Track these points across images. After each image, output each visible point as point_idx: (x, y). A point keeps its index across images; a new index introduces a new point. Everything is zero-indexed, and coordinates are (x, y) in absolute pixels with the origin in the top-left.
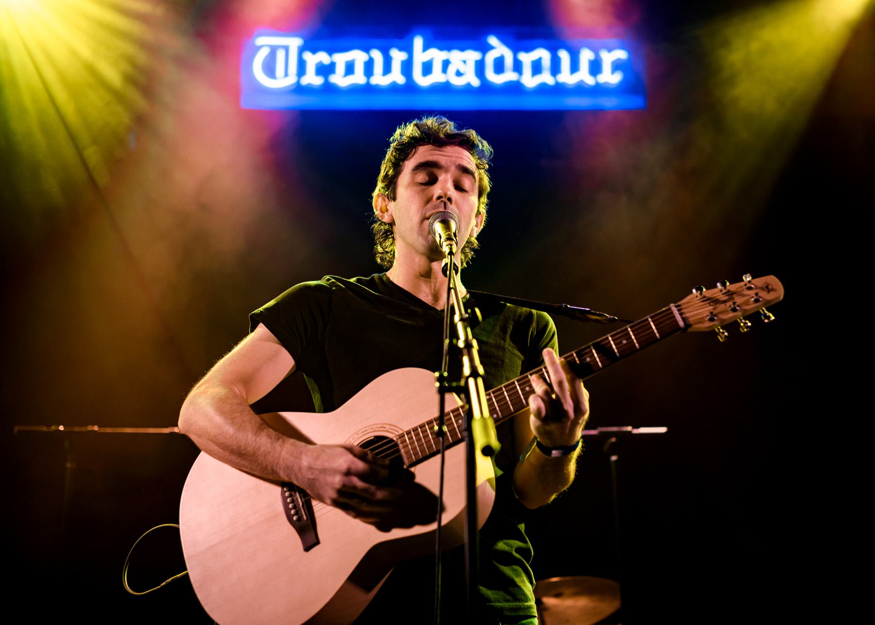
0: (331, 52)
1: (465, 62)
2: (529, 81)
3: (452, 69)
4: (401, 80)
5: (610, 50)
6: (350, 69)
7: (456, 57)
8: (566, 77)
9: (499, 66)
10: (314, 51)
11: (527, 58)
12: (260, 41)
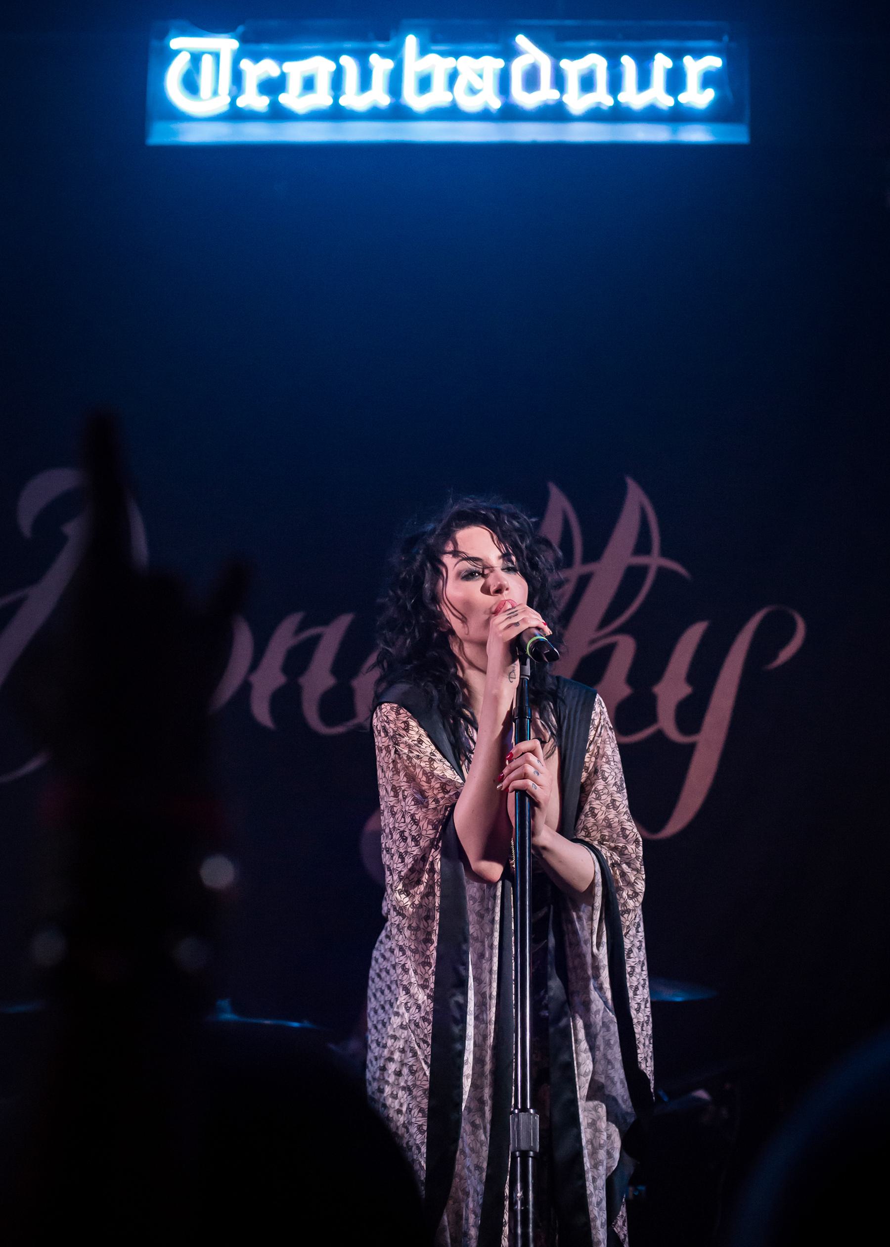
0: (281, 58)
3: (460, 84)
4: (384, 101)
5: (698, 54)
6: (309, 84)
7: (466, 64)
9: (531, 81)
10: (257, 58)
11: (573, 68)
12: (175, 43)
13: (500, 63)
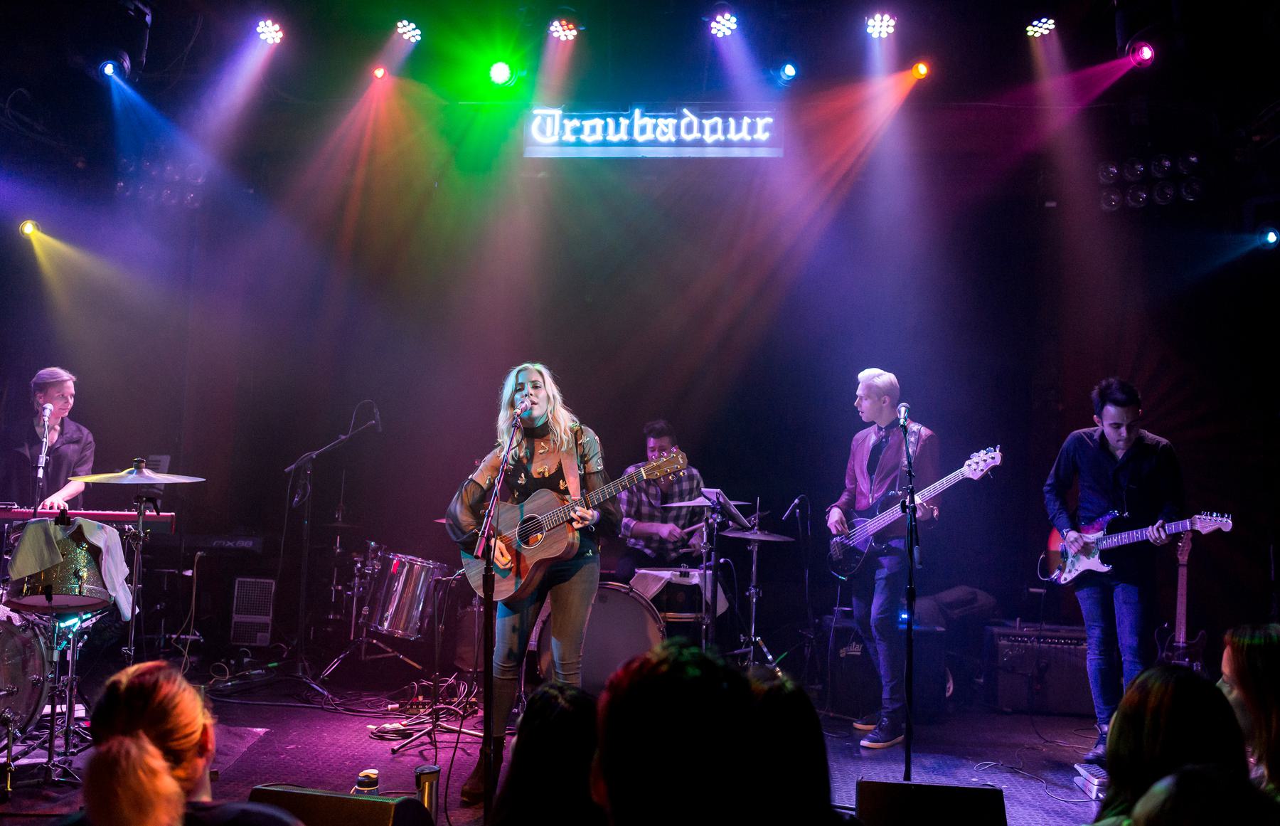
1: (667, 126)
2: (709, 138)
5: (763, 116)
6: (593, 130)
7: (661, 121)
8: (733, 136)
9: (689, 129)
10: (571, 118)
11: (707, 123)
12: (535, 112)
13: (675, 121)
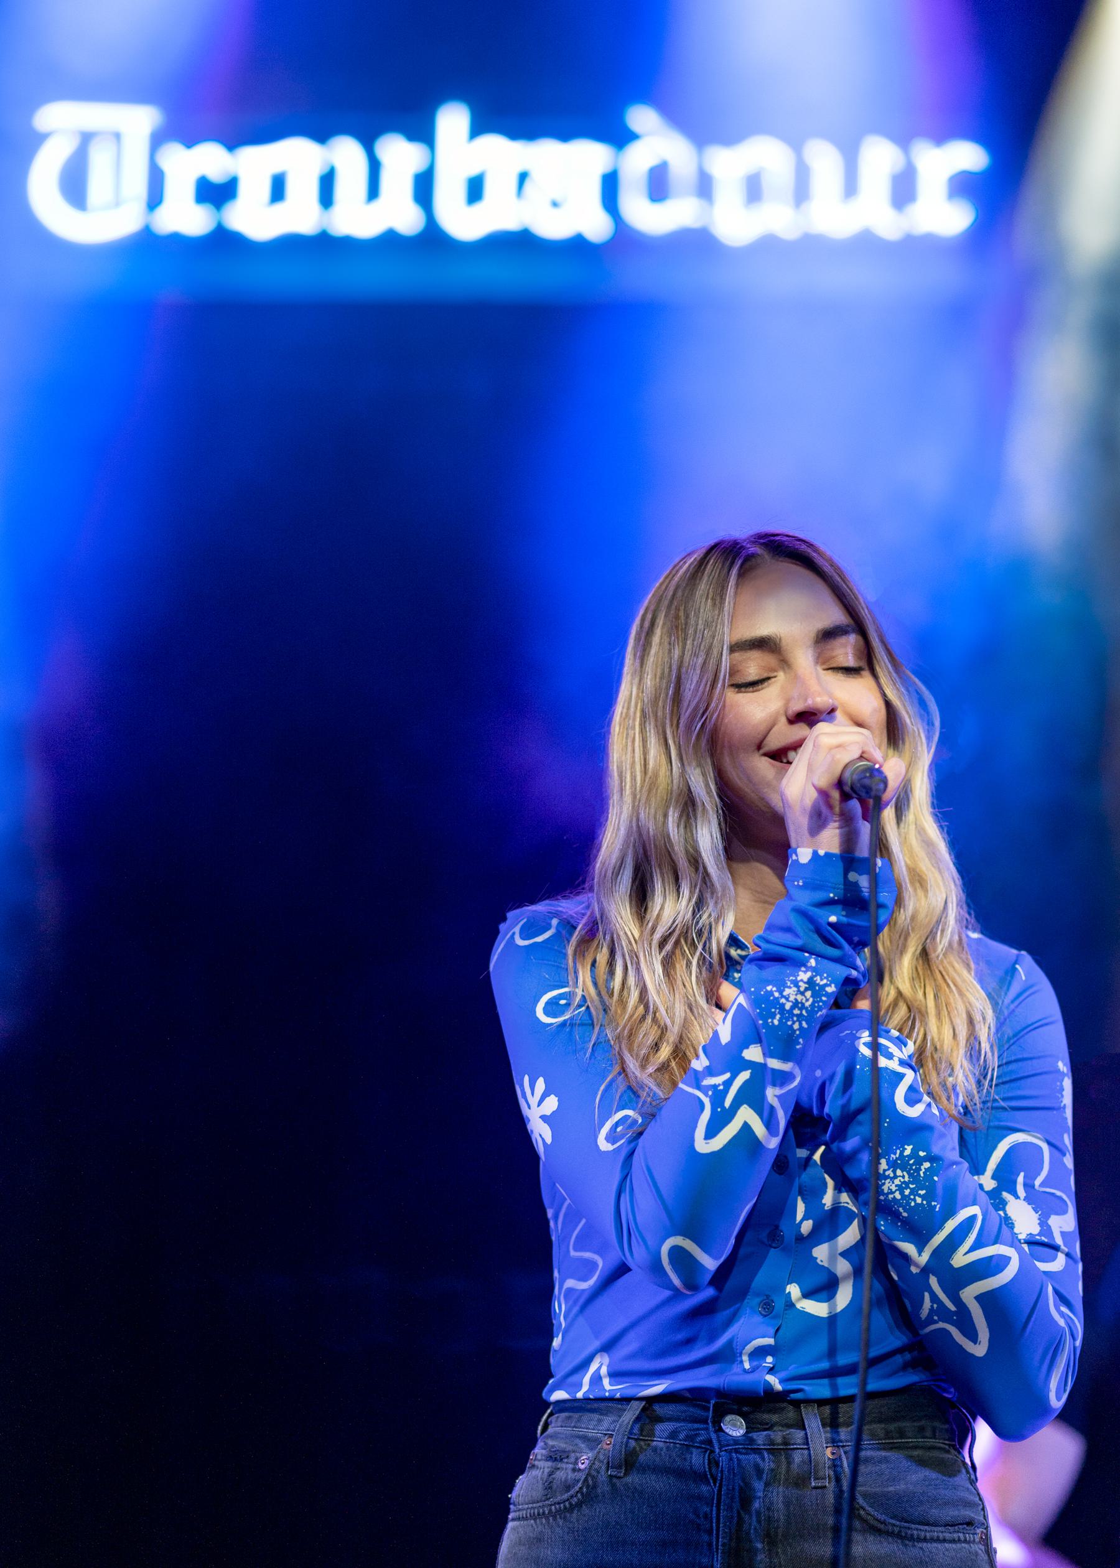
0: (232, 144)
6: (278, 189)
10: (190, 142)
